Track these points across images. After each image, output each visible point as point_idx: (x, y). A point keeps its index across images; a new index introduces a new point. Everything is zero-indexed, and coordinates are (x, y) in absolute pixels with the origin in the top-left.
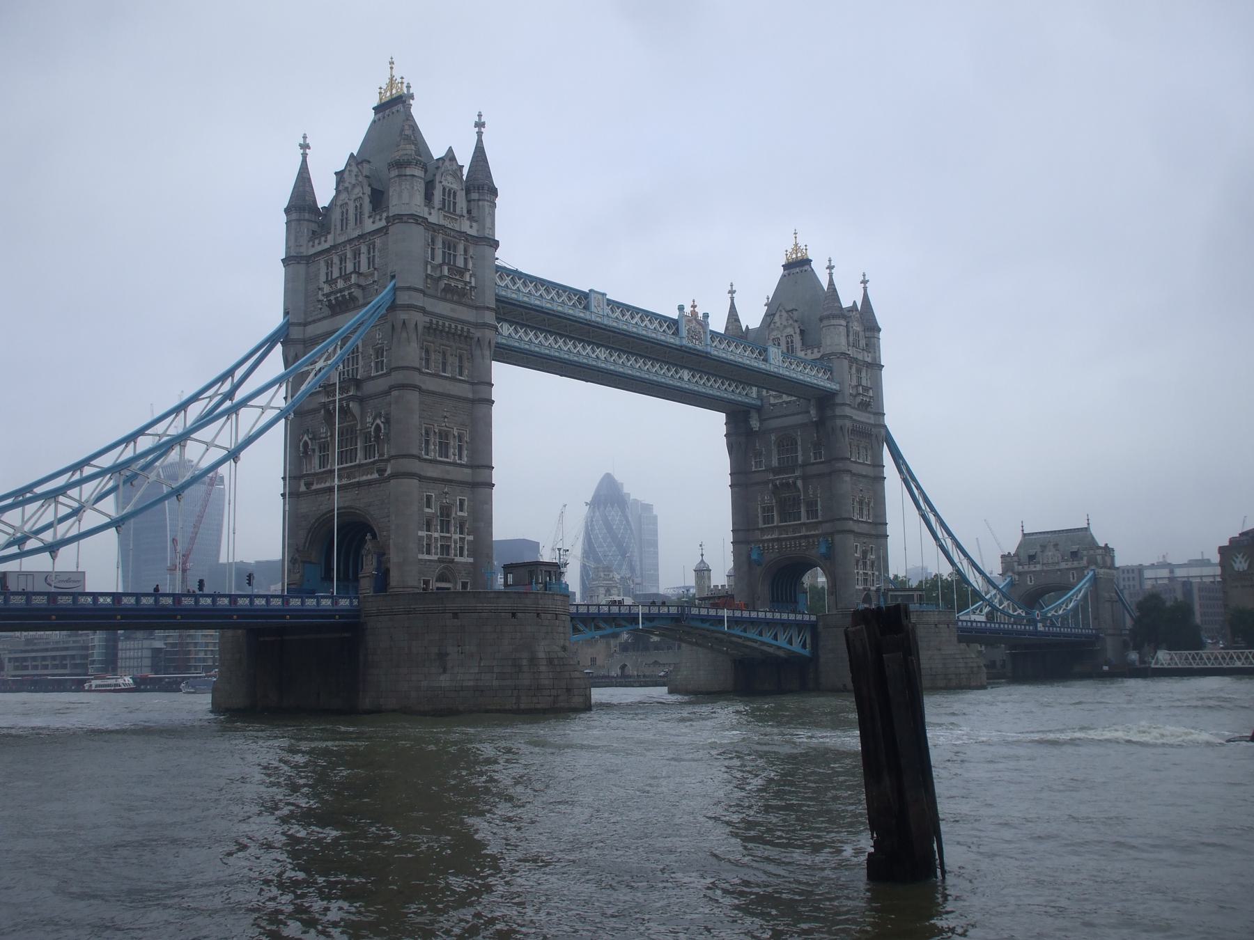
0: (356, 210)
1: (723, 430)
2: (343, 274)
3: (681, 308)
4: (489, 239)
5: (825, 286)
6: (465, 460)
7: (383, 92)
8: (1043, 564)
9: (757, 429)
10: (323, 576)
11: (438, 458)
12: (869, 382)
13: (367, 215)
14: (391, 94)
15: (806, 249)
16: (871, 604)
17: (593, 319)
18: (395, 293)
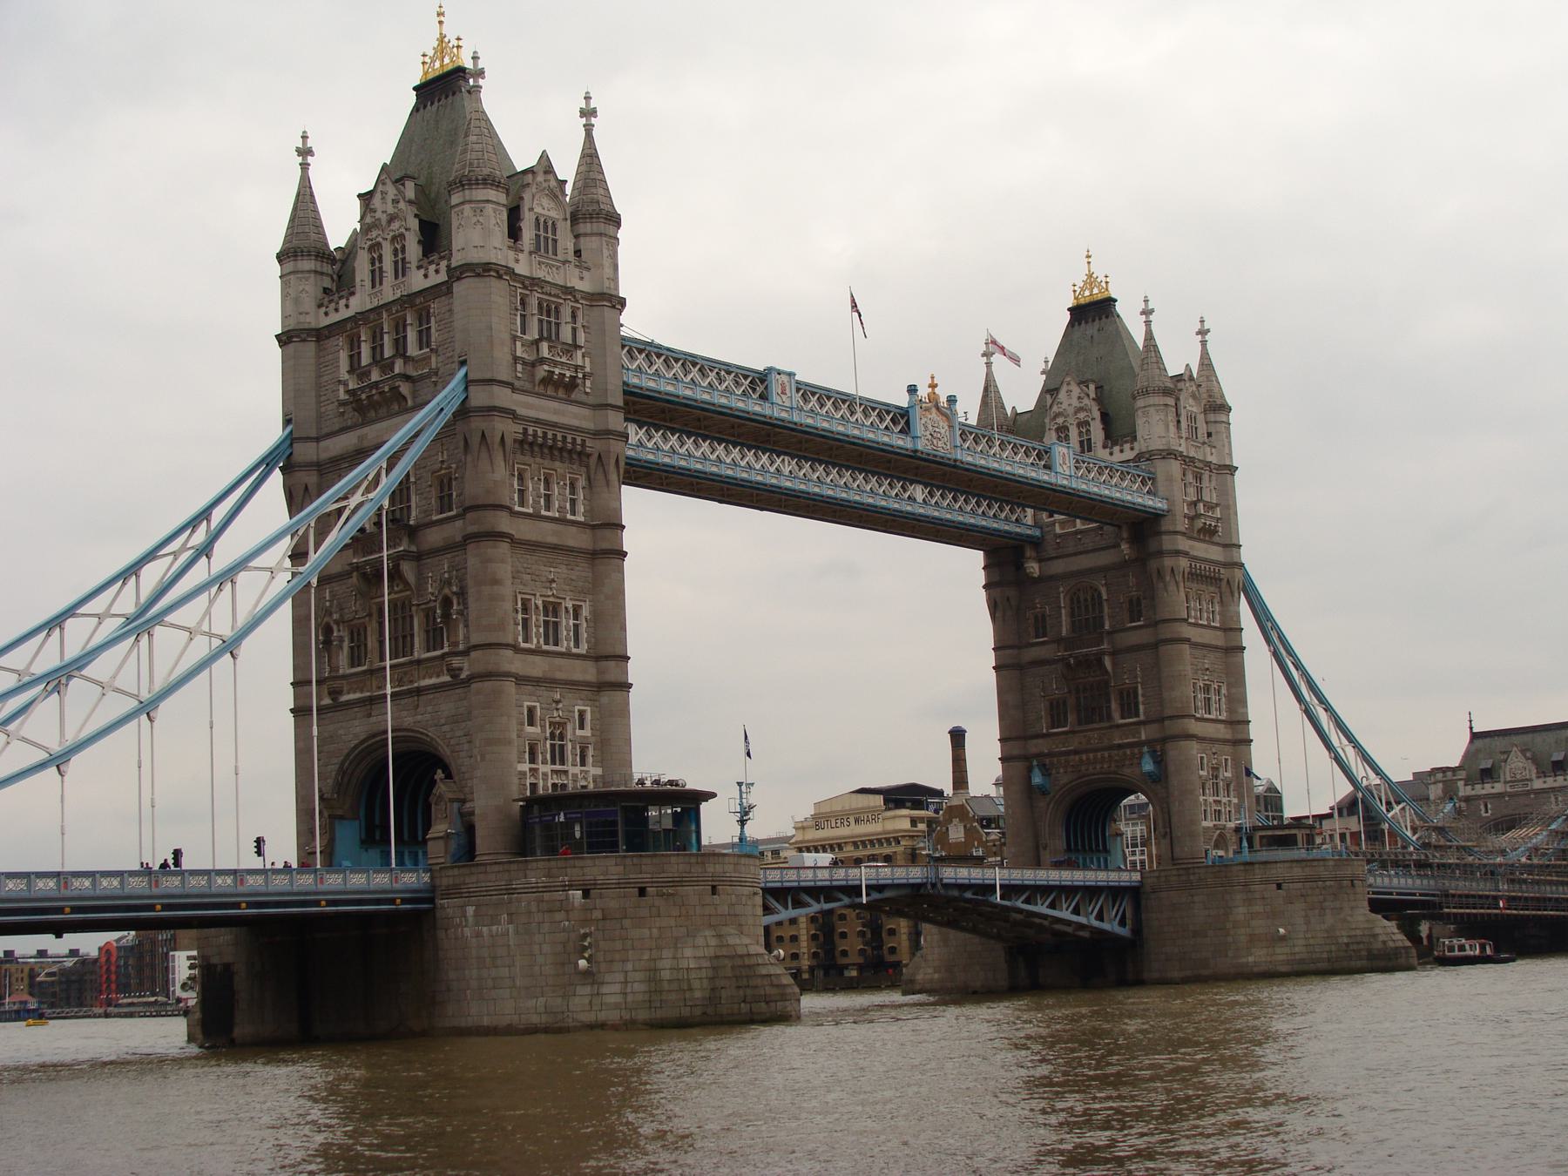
0: (396, 255)
1: (981, 578)
2: (378, 358)
3: (912, 390)
4: (612, 295)
5: (1140, 341)
7: (429, 61)
8: (1506, 782)
9: (1036, 575)
10: (363, 836)
11: (545, 647)
13: (414, 265)
14: (442, 66)
15: (1107, 283)
16: (1227, 851)
17: (776, 415)
18: (466, 388)
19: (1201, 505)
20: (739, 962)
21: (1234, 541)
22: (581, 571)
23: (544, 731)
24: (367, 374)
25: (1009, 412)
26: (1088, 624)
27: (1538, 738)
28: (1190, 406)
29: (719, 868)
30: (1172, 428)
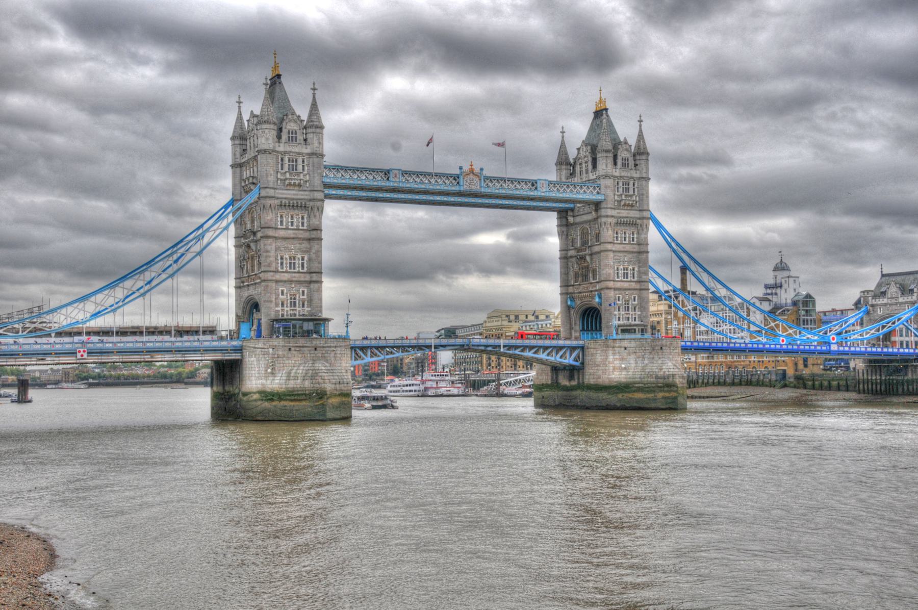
3: (461, 168)
6: (305, 269)
8: (888, 298)
11: (289, 270)
12: (636, 190)
17: (391, 184)
19: (623, 196)
20: (314, 372)
21: (645, 208)
22: (305, 245)
23: (287, 296)
24: (245, 182)
25: (572, 154)
26: (584, 243)
27: (908, 277)
28: (622, 154)
29: (318, 343)
30: (610, 166)
